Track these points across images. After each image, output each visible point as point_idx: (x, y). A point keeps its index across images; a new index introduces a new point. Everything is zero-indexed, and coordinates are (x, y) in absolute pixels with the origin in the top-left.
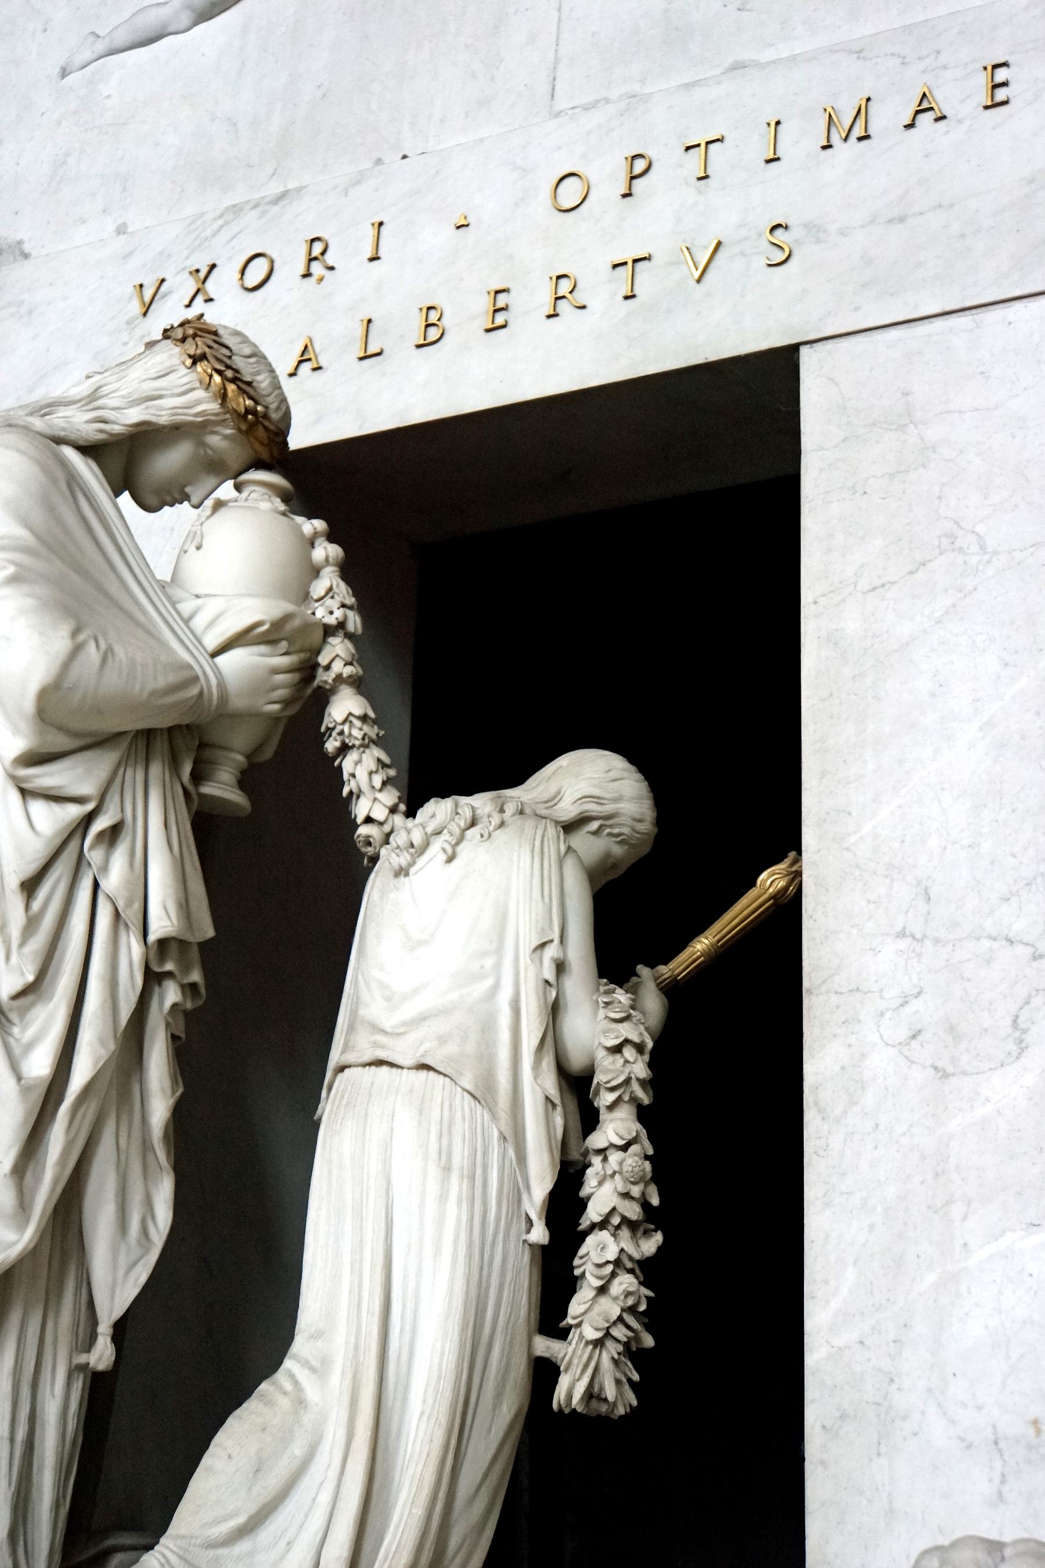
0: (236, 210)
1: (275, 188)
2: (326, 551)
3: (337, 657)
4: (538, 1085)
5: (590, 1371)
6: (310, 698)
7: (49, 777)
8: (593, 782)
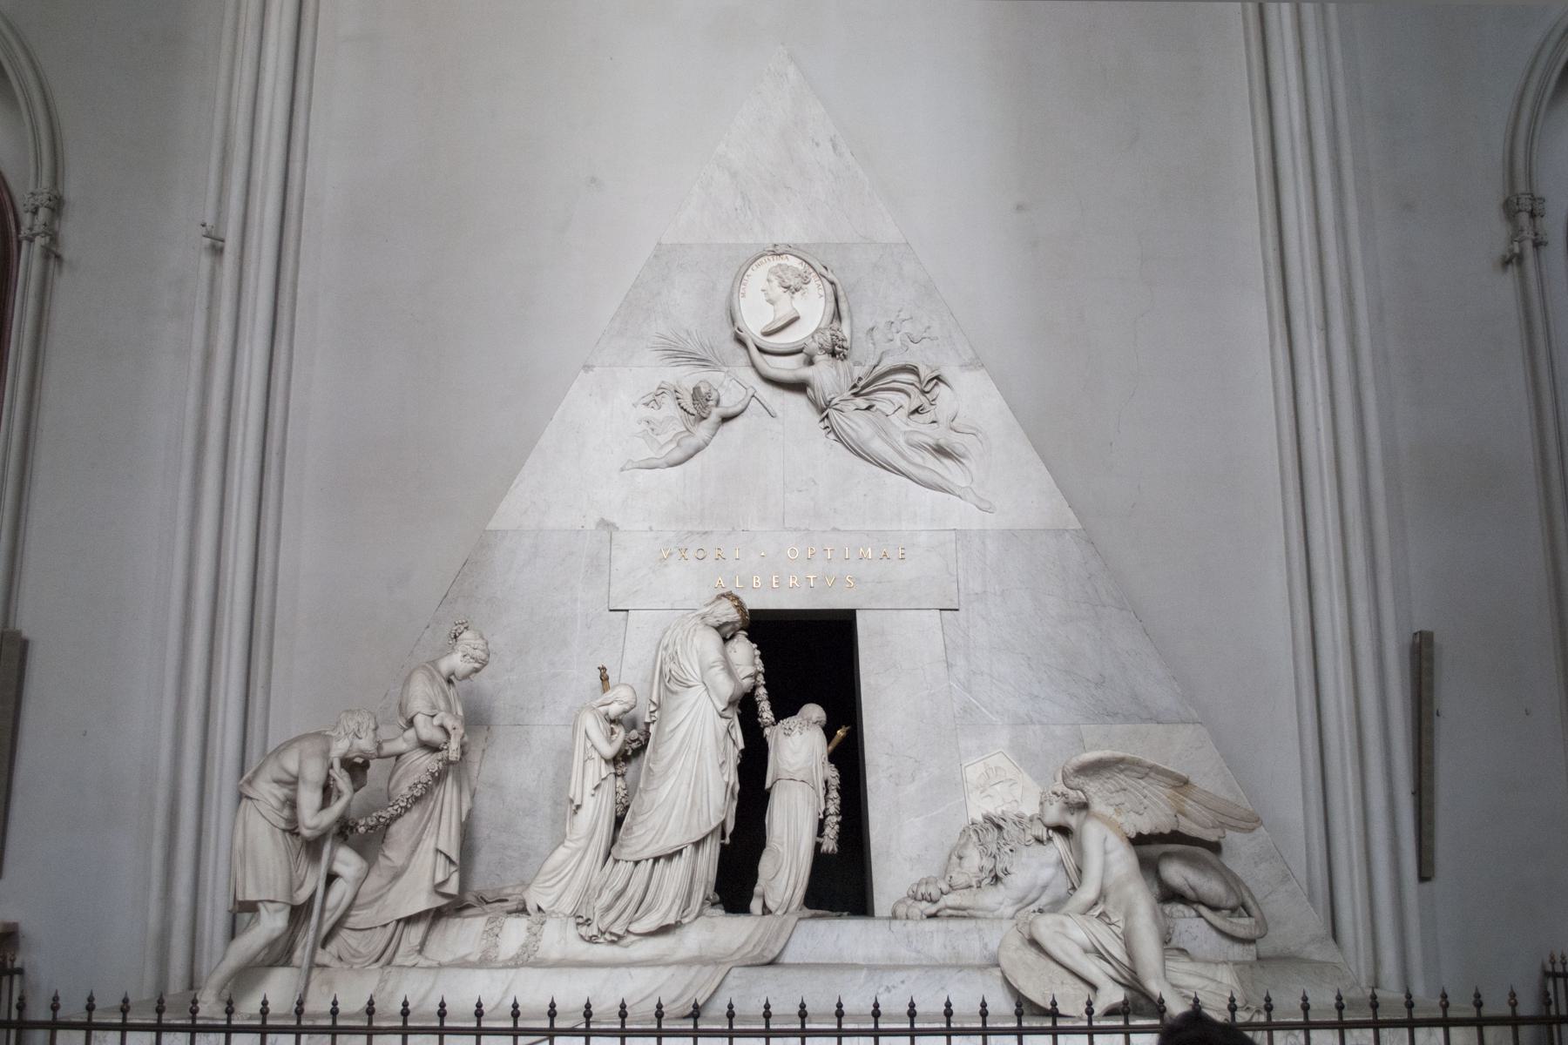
0: (692, 533)
1: (701, 529)
2: (758, 652)
3: (761, 678)
4: (821, 785)
5: (830, 845)
6: (755, 688)
7: (727, 714)
8: (814, 712)
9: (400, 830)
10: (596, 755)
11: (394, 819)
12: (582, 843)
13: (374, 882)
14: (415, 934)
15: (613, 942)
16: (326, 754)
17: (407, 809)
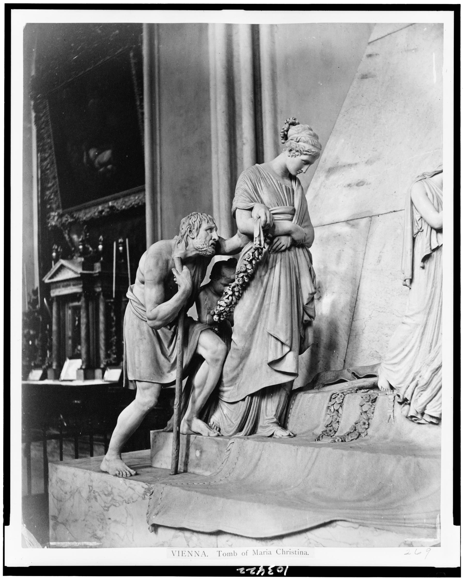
9: (240, 316)
10: (425, 227)
11: (232, 306)
12: (420, 319)
13: (230, 363)
14: (270, 407)
15: (431, 423)
16: (170, 252)
17: (239, 298)
